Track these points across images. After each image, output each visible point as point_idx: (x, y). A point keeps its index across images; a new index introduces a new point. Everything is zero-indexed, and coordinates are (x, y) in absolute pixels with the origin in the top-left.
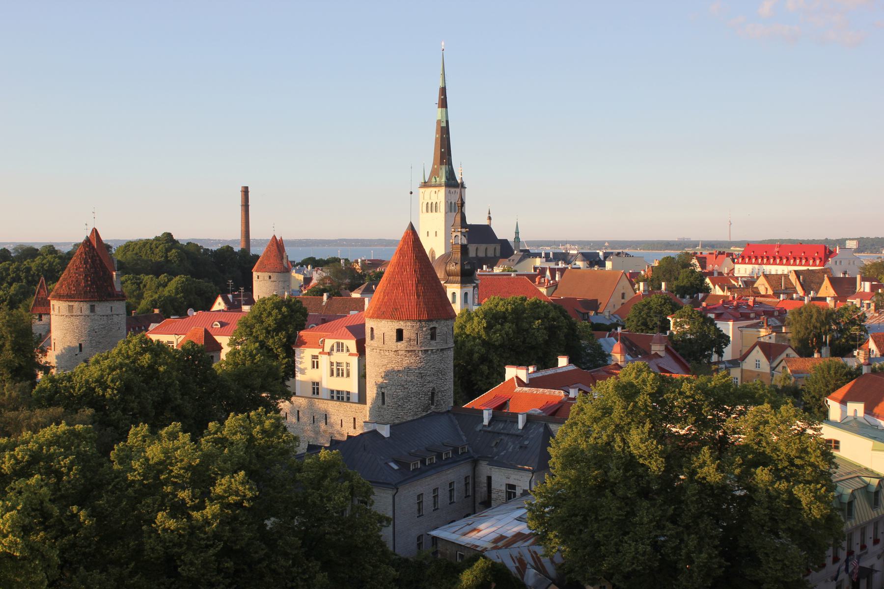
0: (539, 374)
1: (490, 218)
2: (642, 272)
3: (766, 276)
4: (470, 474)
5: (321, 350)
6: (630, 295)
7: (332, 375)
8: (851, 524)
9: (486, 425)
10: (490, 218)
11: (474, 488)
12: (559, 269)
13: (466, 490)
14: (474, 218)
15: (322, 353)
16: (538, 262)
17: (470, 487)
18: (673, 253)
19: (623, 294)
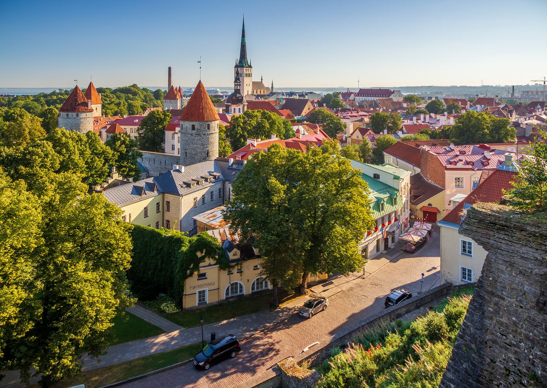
0: (262, 142)
1: (262, 79)
2: (320, 100)
3: (366, 101)
4: (222, 187)
5: (174, 132)
6: (312, 108)
7: (179, 142)
8: (383, 214)
9: (230, 166)
10: (262, 79)
11: (223, 193)
12: (285, 99)
13: (220, 195)
14: (256, 78)
15: (175, 133)
16: (280, 96)
17: (222, 193)
18: (331, 93)
19: (309, 108)
